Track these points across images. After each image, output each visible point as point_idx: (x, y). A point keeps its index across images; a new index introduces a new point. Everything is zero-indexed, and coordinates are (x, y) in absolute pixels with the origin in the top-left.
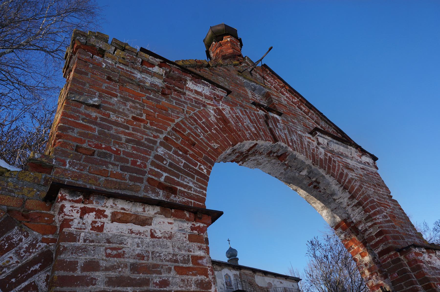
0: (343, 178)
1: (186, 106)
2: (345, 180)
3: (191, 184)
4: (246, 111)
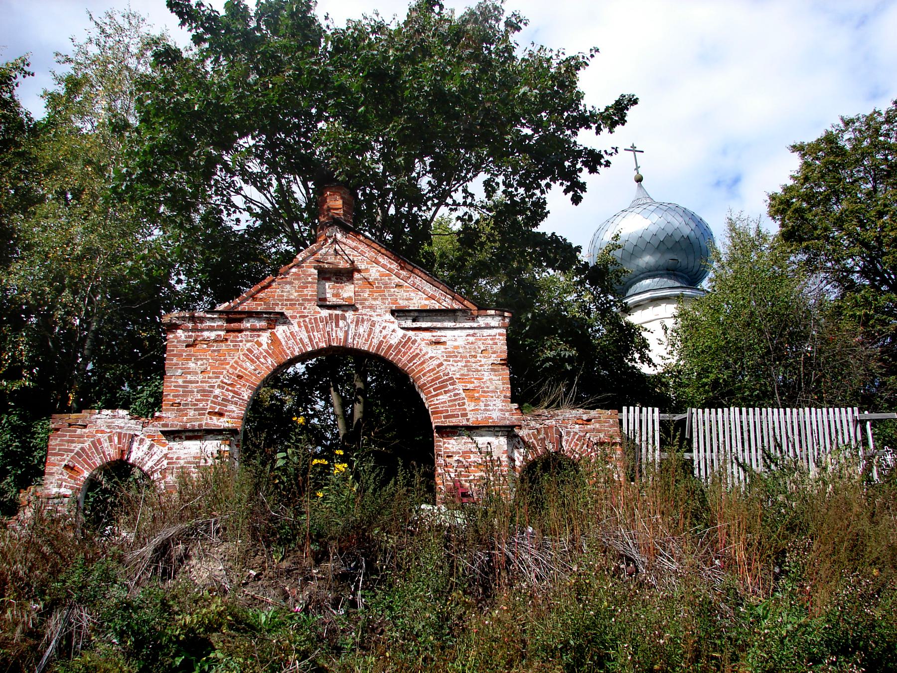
0: (415, 361)
1: (241, 344)
2: (414, 364)
3: (235, 409)
4: (304, 321)
